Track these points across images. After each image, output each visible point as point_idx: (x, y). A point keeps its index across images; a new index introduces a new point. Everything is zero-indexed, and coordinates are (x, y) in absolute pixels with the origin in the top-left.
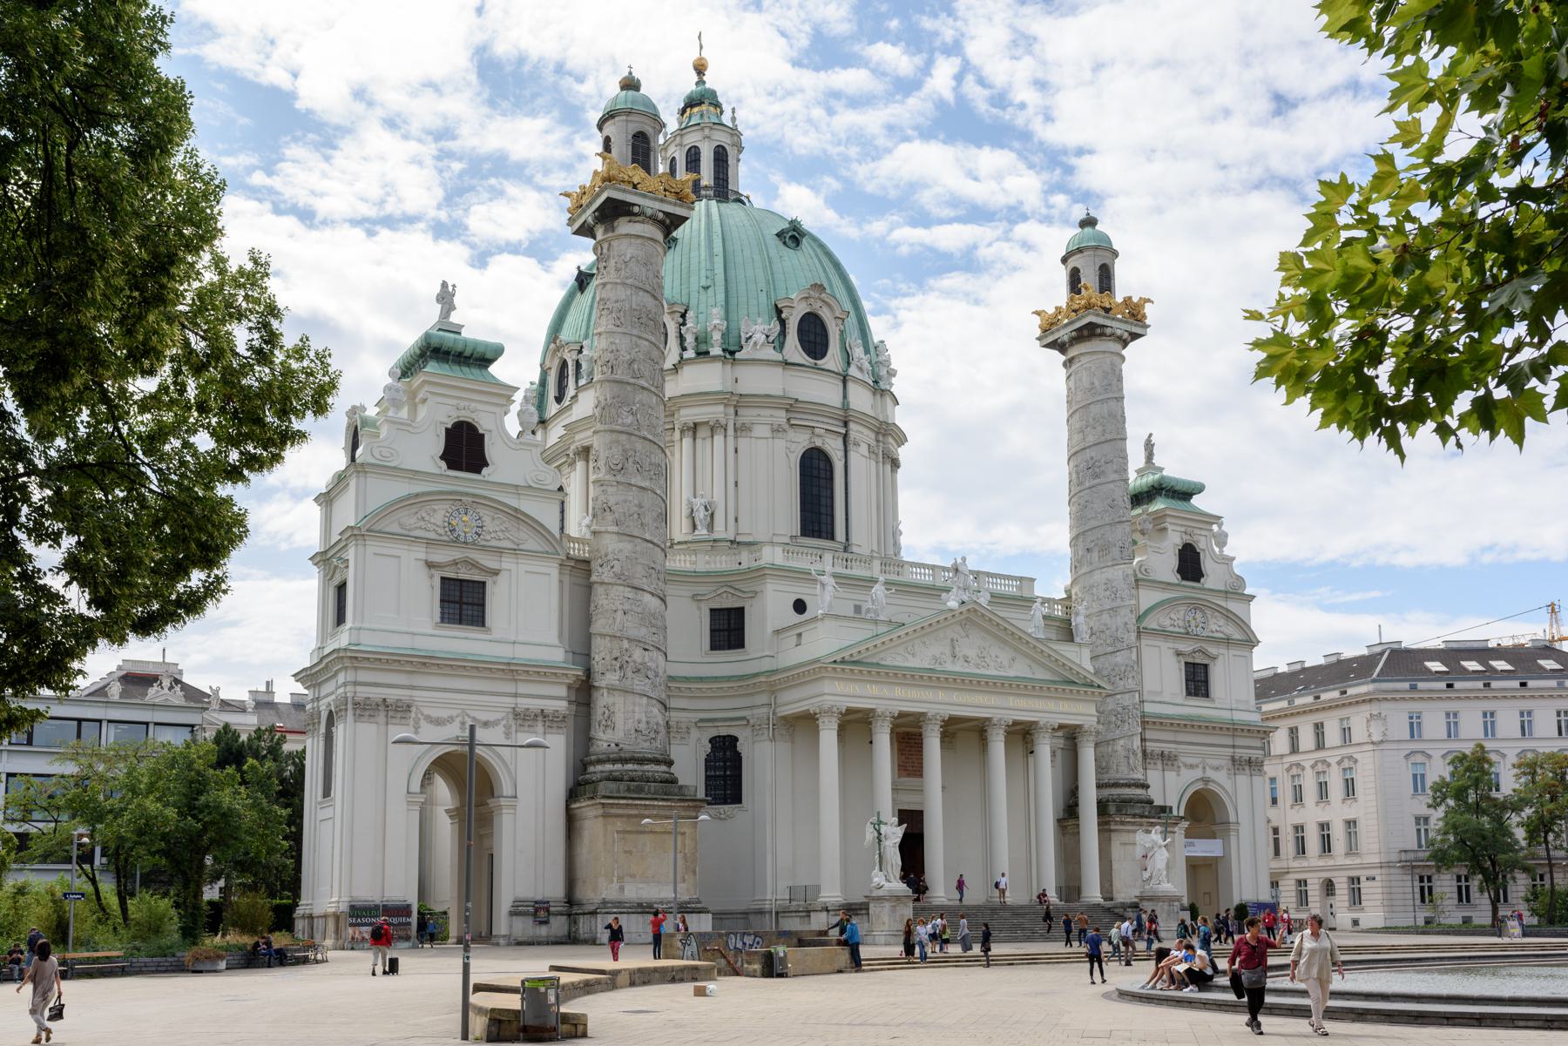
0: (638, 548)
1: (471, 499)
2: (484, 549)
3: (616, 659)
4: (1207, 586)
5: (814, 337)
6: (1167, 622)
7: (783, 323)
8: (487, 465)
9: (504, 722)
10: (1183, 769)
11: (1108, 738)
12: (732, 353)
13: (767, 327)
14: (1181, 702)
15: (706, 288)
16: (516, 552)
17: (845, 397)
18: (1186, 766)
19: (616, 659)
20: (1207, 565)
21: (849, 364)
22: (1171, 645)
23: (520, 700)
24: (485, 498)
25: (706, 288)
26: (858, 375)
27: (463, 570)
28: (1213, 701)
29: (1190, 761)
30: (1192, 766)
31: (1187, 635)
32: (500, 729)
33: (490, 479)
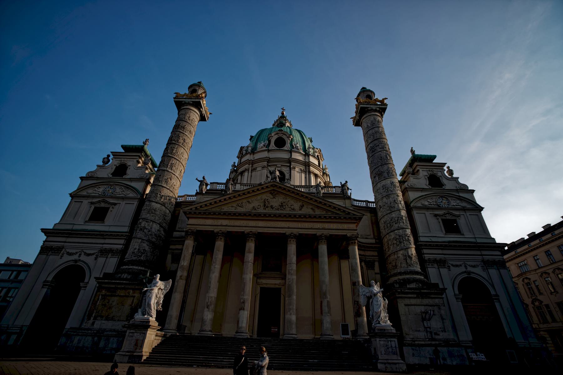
0: (156, 188)
1: (113, 183)
4: (446, 188)
5: (280, 143)
6: (427, 203)
9: (97, 254)
10: (451, 267)
11: (394, 251)
13: (264, 143)
14: (444, 236)
16: (123, 198)
17: (291, 156)
18: (453, 265)
20: (444, 181)
22: (432, 212)
23: (104, 245)
24: (116, 182)
26: (296, 150)
27: (103, 204)
28: (463, 235)
30: (457, 266)
31: (439, 208)
32: (94, 256)
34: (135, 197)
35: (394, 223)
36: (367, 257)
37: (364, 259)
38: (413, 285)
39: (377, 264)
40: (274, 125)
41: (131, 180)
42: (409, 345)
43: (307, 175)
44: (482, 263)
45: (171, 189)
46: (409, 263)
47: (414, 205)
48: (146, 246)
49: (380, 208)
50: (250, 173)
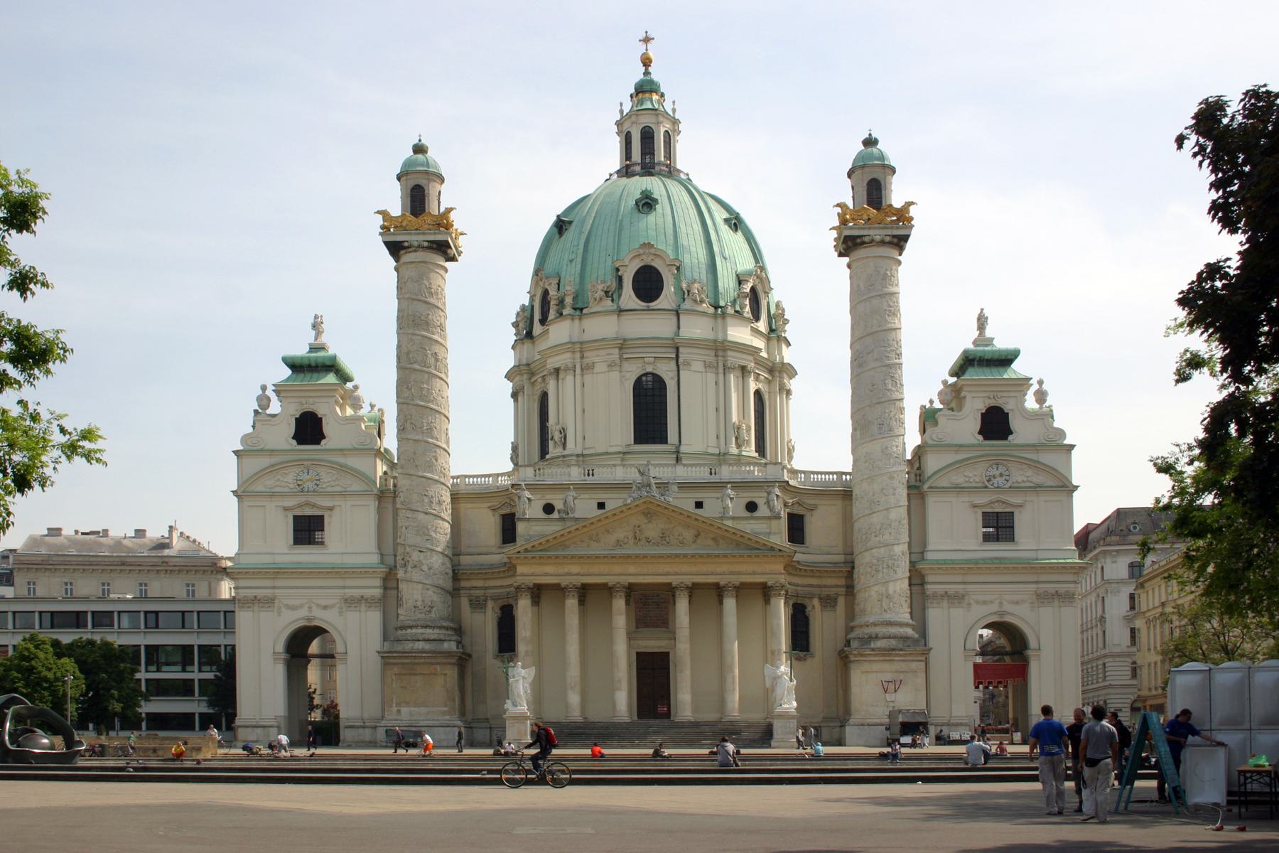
1: (310, 463)
2: (321, 494)
3: (403, 559)
7: (620, 279)
8: (324, 437)
12: (581, 310)
15: (571, 261)
16: (343, 494)
18: (977, 602)
19: (403, 559)
21: (684, 299)
24: (319, 460)
25: (571, 261)
29: (982, 598)
30: (985, 602)
33: (327, 447)
34: (367, 491)
35: (873, 535)
36: (823, 589)
37: (819, 593)
38: (880, 644)
39: (841, 601)
40: (622, 124)
41: (342, 451)
42: (855, 725)
43: (721, 377)
44: (1034, 597)
45: (442, 480)
46: (886, 608)
47: (934, 485)
48: (433, 596)
49: (857, 500)
50: (578, 377)
